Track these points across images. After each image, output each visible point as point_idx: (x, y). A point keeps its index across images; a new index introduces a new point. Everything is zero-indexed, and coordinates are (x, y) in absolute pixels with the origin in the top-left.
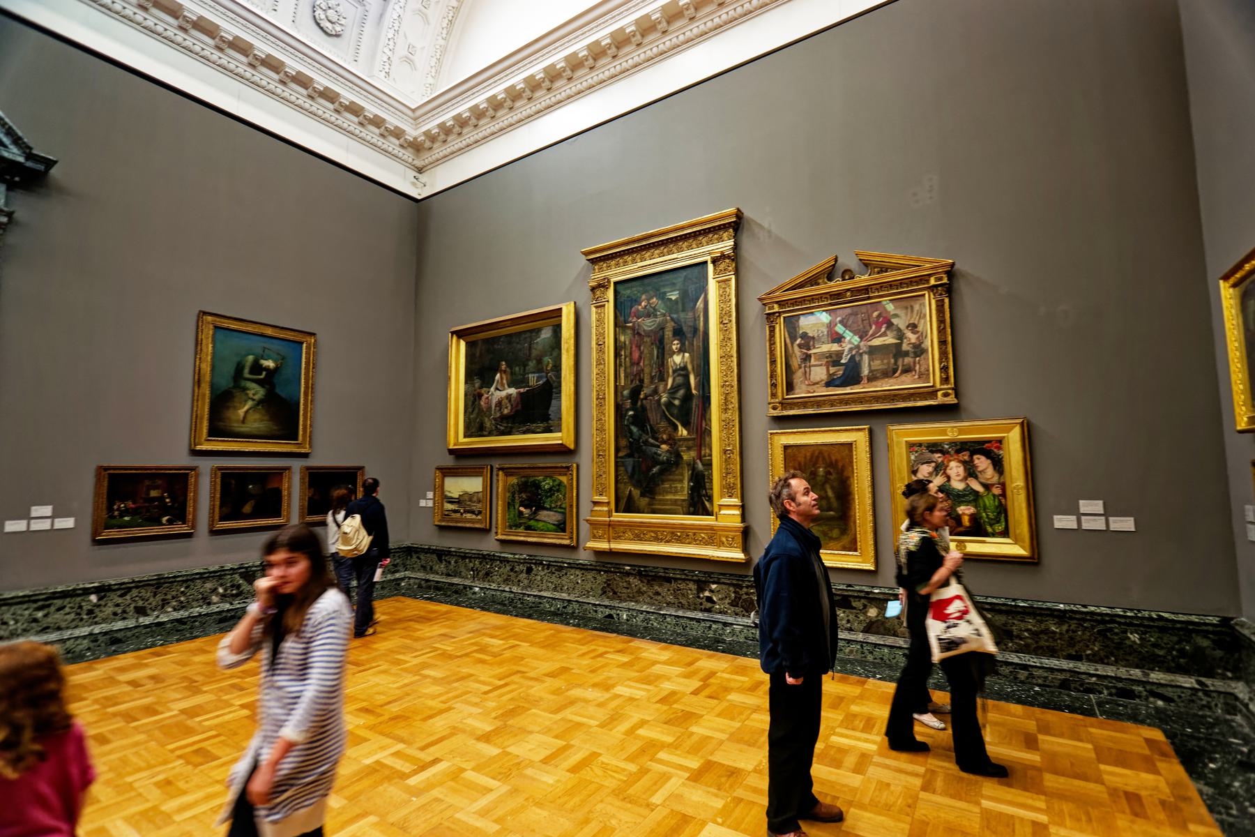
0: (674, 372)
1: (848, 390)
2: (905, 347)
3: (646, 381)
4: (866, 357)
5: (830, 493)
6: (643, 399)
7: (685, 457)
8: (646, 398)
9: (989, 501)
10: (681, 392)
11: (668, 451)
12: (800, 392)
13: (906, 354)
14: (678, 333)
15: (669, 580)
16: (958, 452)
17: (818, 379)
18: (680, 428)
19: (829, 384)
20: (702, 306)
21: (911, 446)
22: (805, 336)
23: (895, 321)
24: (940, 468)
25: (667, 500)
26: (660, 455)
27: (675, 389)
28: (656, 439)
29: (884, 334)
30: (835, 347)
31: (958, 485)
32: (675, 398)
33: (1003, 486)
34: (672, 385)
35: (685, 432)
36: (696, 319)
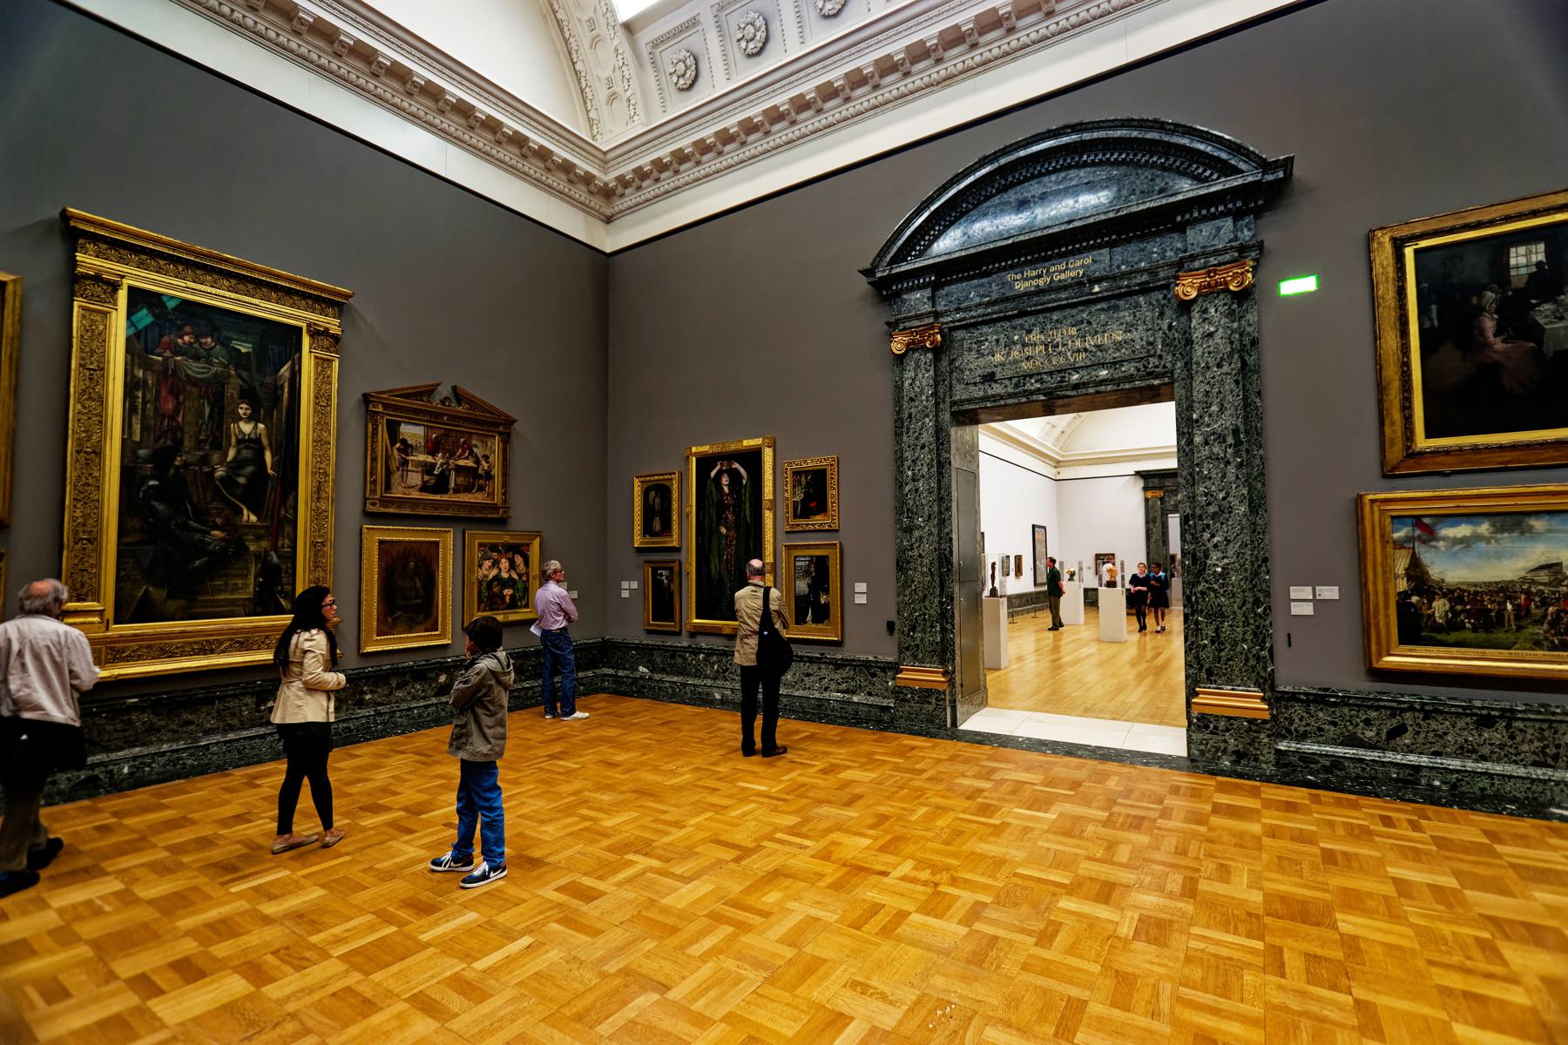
0: (239, 442)
1: (438, 497)
2: (480, 471)
3: (187, 444)
4: (453, 473)
5: (418, 584)
6: (178, 468)
7: (252, 548)
8: (186, 465)
9: (520, 585)
10: (249, 469)
11: (223, 539)
12: (397, 492)
13: (480, 477)
14: (247, 394)
15: (209, 701)
16: (506, 552)
17: (413, 483)
18: (245, 512)
19: (424, 488)
20: (287, 374)
21: (480, 545)
22: (404, 441)
23: (475, 450)
24: (496, 564)
25: (218, 601)
26: (209, 544)
27: (237, 465)
28: (204, 523)
29: (467, 458)
30: (430, 459)
31: (505, 575)
32: (240, 475)
33: (528, 574)
34: (234, 459)
35: (253, 518)
36: (278, 388)
